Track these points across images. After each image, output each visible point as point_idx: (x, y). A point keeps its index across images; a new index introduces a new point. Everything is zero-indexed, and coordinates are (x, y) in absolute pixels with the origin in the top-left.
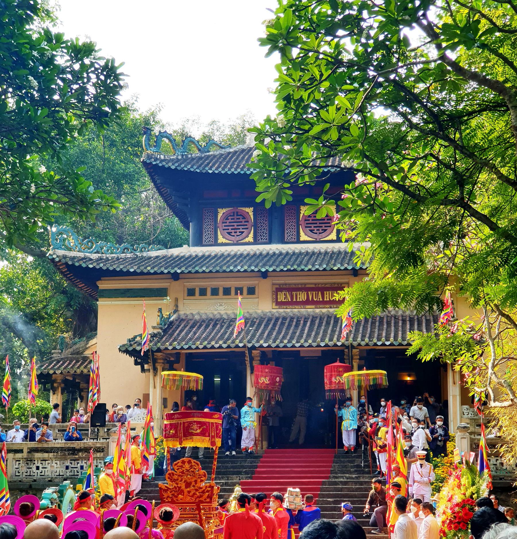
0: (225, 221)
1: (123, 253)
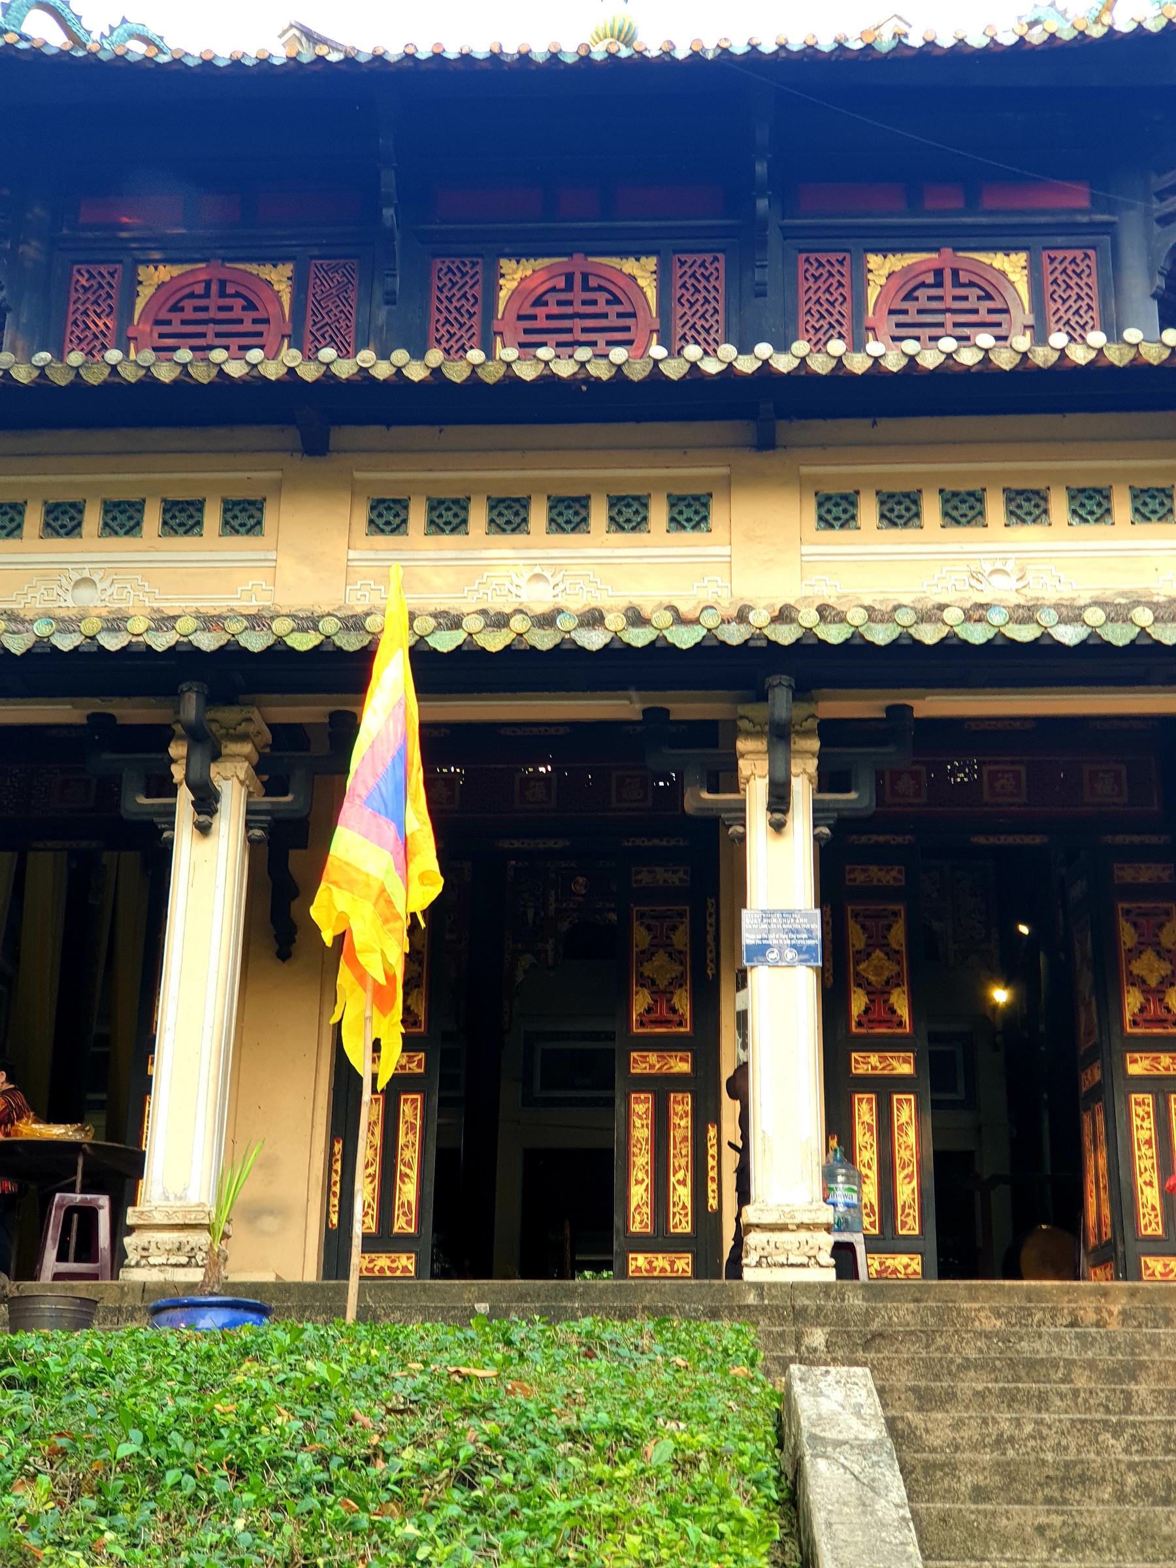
0: (164, 315)
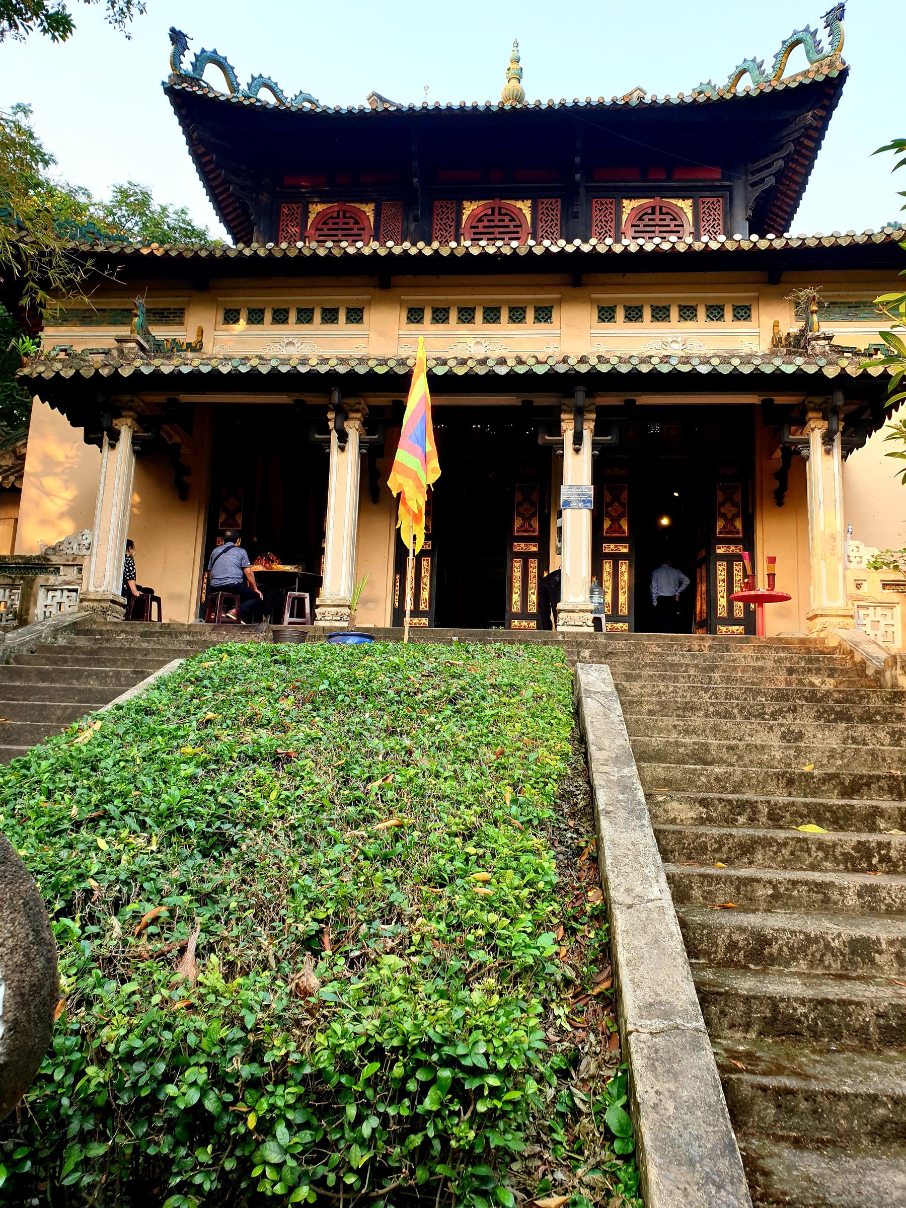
0: (320, 226)
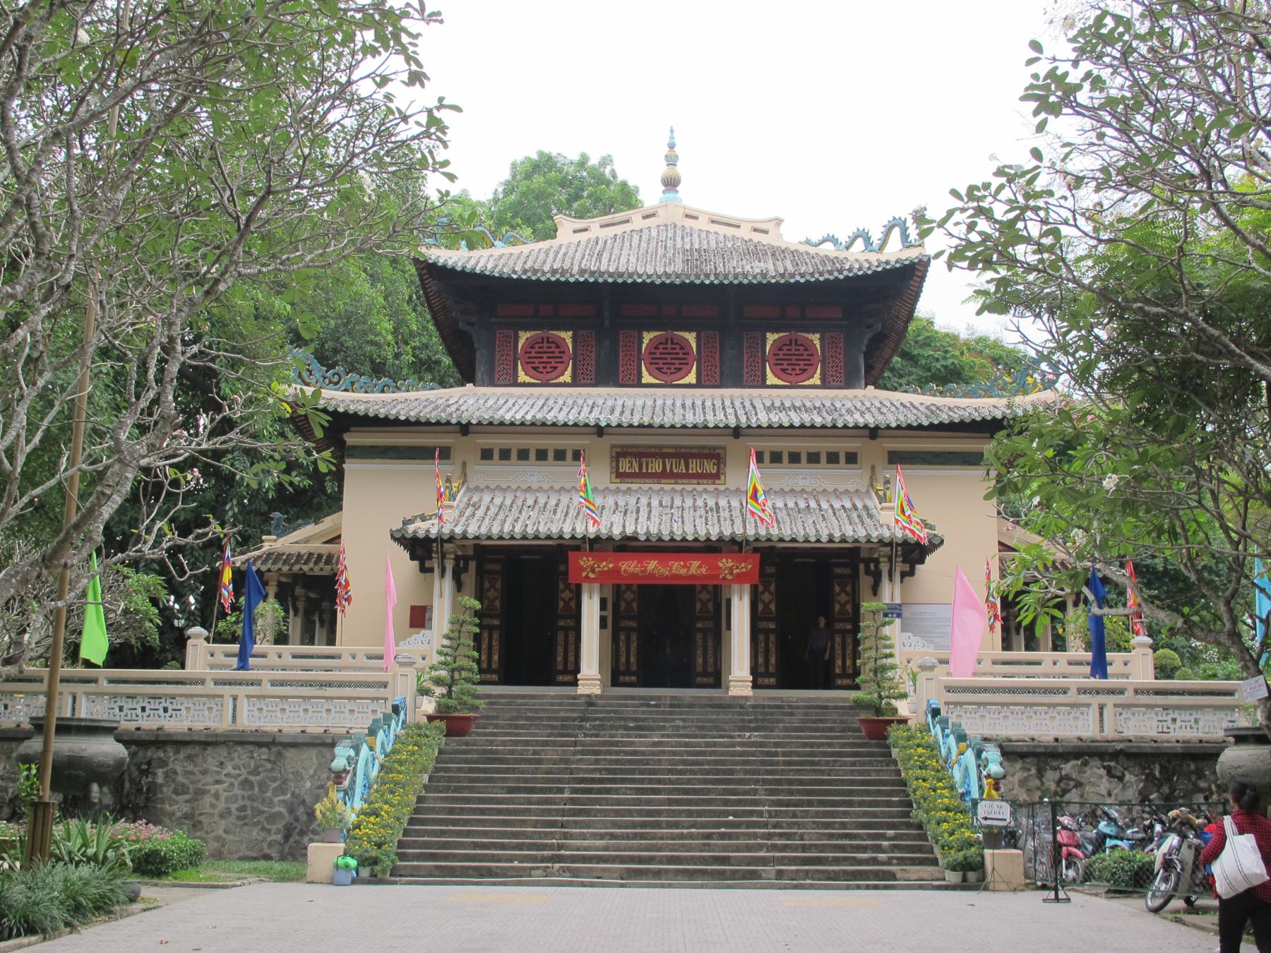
1: (383, 391)
